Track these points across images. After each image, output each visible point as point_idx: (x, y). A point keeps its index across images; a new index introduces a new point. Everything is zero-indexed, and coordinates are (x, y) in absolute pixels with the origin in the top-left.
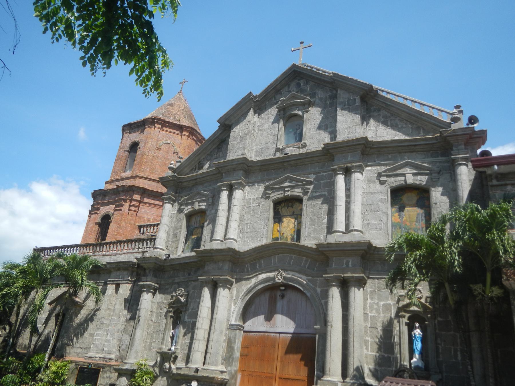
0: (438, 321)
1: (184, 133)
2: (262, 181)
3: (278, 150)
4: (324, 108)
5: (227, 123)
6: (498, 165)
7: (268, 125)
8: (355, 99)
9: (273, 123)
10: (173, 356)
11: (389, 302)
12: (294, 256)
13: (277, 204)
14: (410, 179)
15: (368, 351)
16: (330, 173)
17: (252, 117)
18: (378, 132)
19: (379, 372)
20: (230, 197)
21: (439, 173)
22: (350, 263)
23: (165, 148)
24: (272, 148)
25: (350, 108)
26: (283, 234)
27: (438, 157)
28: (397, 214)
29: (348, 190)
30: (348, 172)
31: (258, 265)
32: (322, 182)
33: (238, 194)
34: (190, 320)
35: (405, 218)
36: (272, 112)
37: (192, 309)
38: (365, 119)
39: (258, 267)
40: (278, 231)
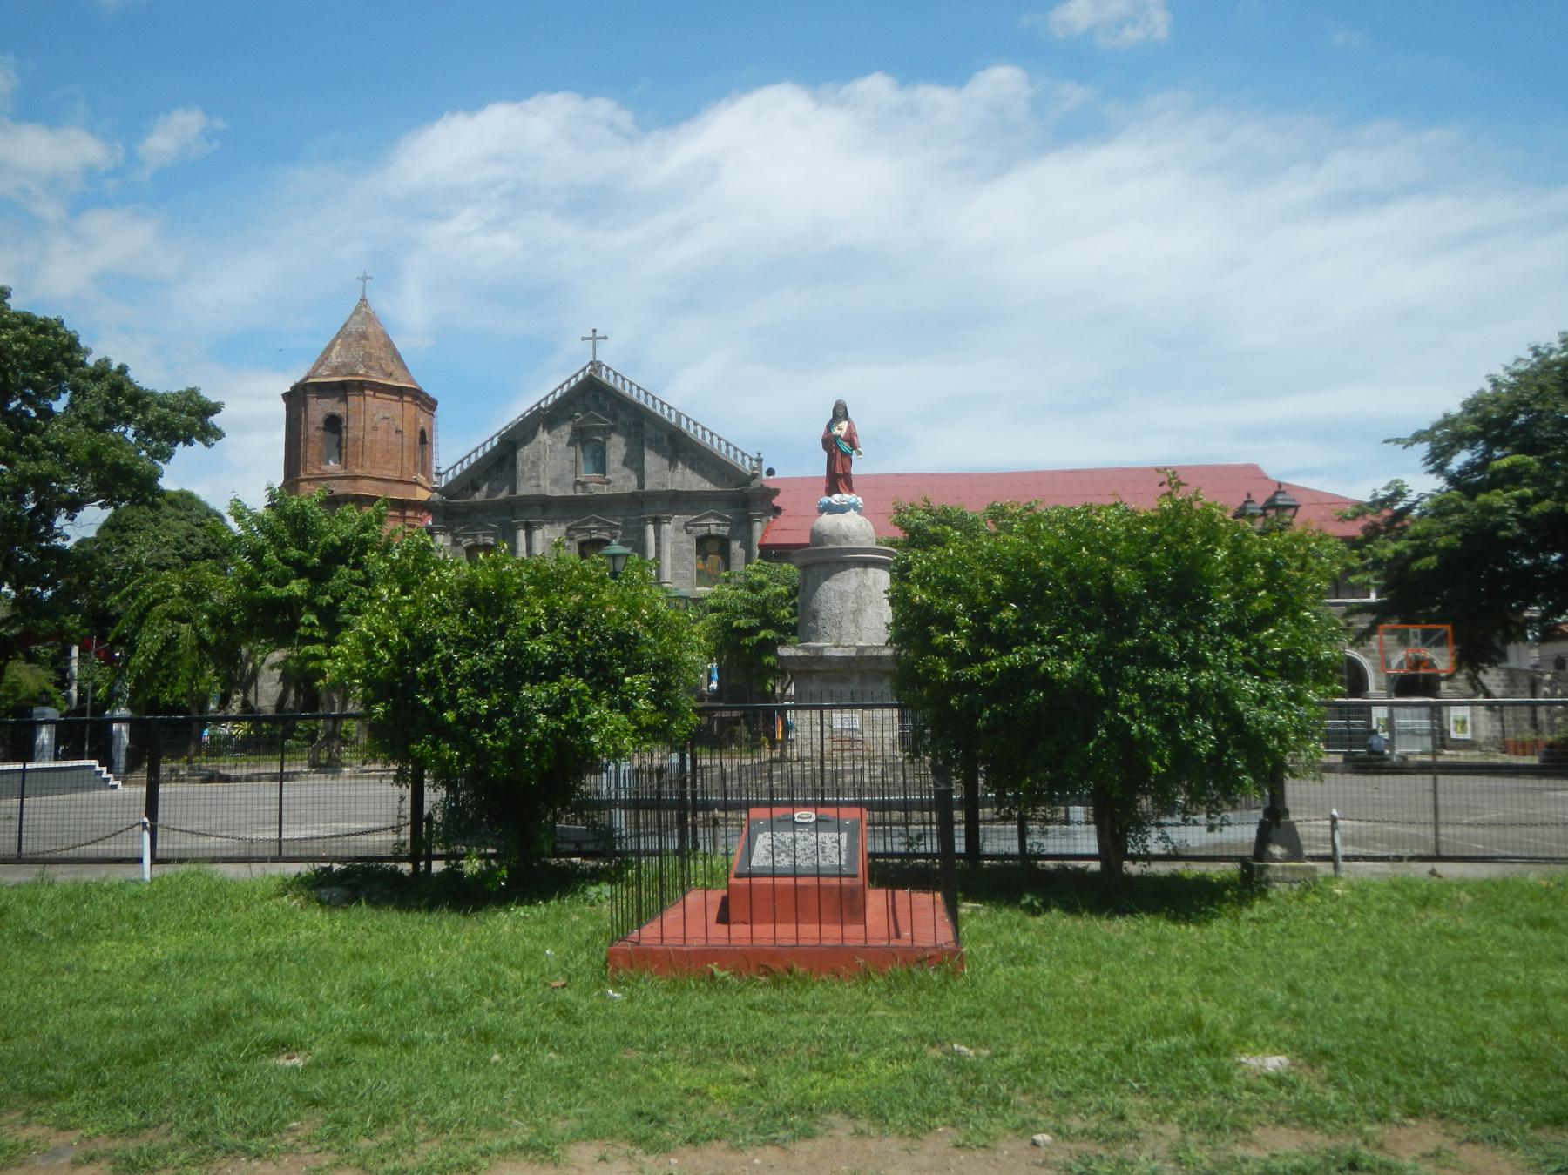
1: (406, 399)
2: (561, 520)
3: (578, 482)
4: (627, 436)
7: (562, 445)
9: (569, 444)
13: (582, 545)
14: (714, 530)
17: (543, 436)
18: (686, 480)
20: (529, 536)
23: (383, 425)
24: (571, 479)
25: (659, 450)
29: (658, 538)
30: (657, 522)
33: (538, 535)
36: (566, 430)
38: (672, 464)
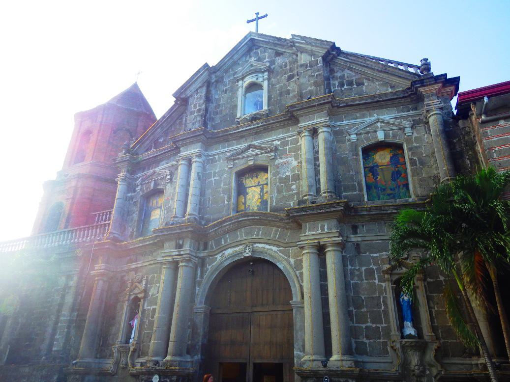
0: (429, 283)
5: (183, 96)
6: (488, 97)
8: (317, 60)
10: (132, 349)
11: (371, 266)
12: (262, 227)
15: (353, 323)
16: (295, 137)
19: (368, 345)
21: (412, 128)
22: (326, 227)
26: (249, 206)
27: (409, 111)
28: (371, 174)
31: (223, 240)
32: (287, 147)
34: (149, 308)
35: (379, 177)
37: (152, 295)
39: (223, 243)
40: (243, 204)
